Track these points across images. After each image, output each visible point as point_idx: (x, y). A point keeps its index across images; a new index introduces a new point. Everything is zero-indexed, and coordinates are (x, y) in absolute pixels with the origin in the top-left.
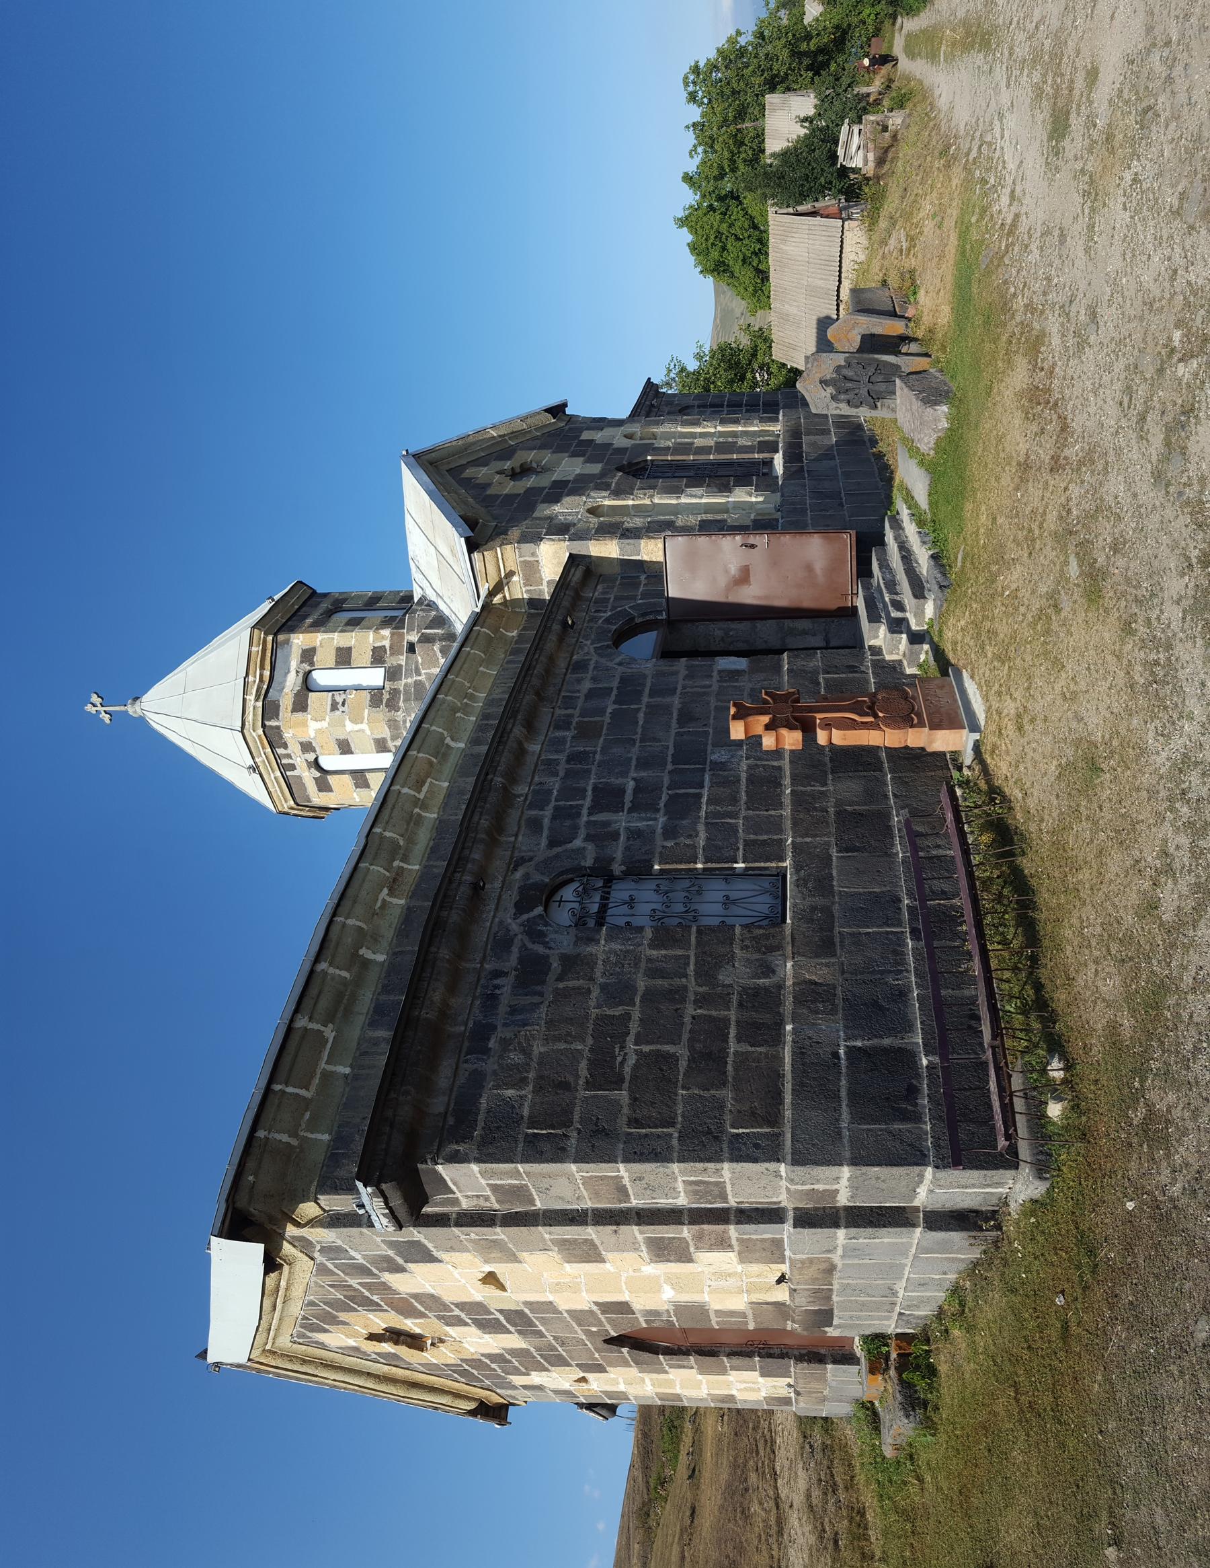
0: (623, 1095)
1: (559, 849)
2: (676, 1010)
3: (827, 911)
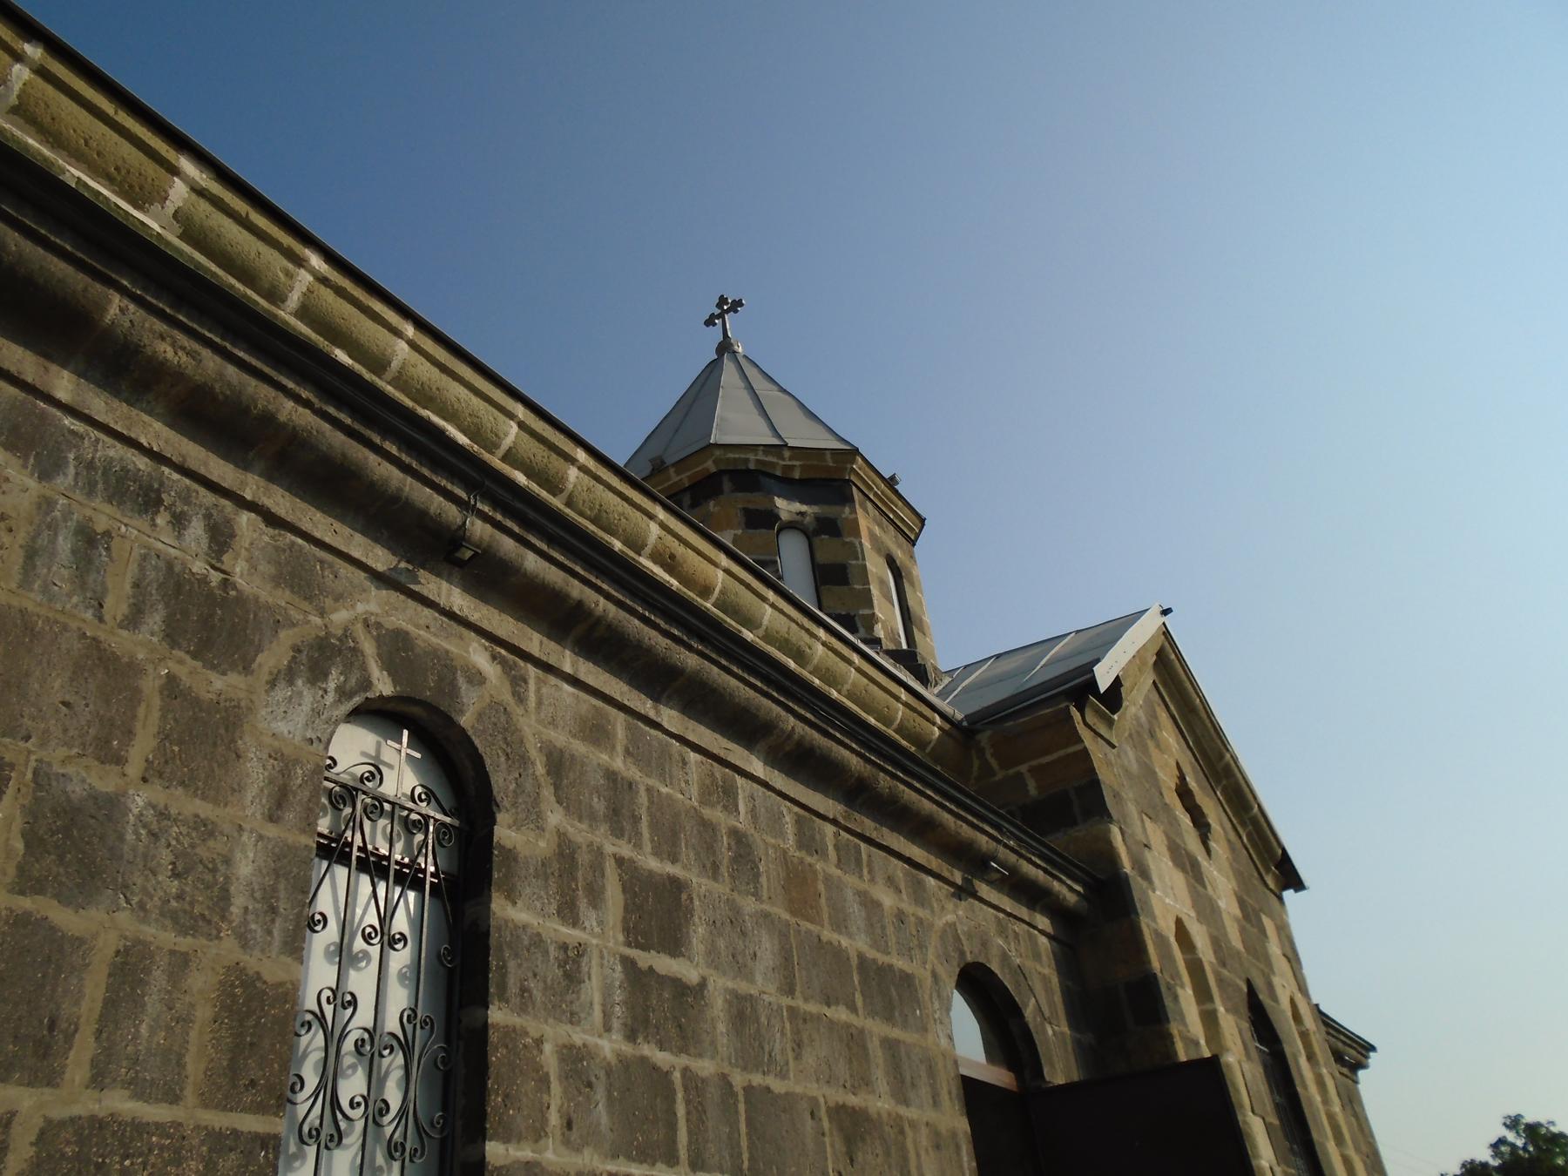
1: (540, 769)
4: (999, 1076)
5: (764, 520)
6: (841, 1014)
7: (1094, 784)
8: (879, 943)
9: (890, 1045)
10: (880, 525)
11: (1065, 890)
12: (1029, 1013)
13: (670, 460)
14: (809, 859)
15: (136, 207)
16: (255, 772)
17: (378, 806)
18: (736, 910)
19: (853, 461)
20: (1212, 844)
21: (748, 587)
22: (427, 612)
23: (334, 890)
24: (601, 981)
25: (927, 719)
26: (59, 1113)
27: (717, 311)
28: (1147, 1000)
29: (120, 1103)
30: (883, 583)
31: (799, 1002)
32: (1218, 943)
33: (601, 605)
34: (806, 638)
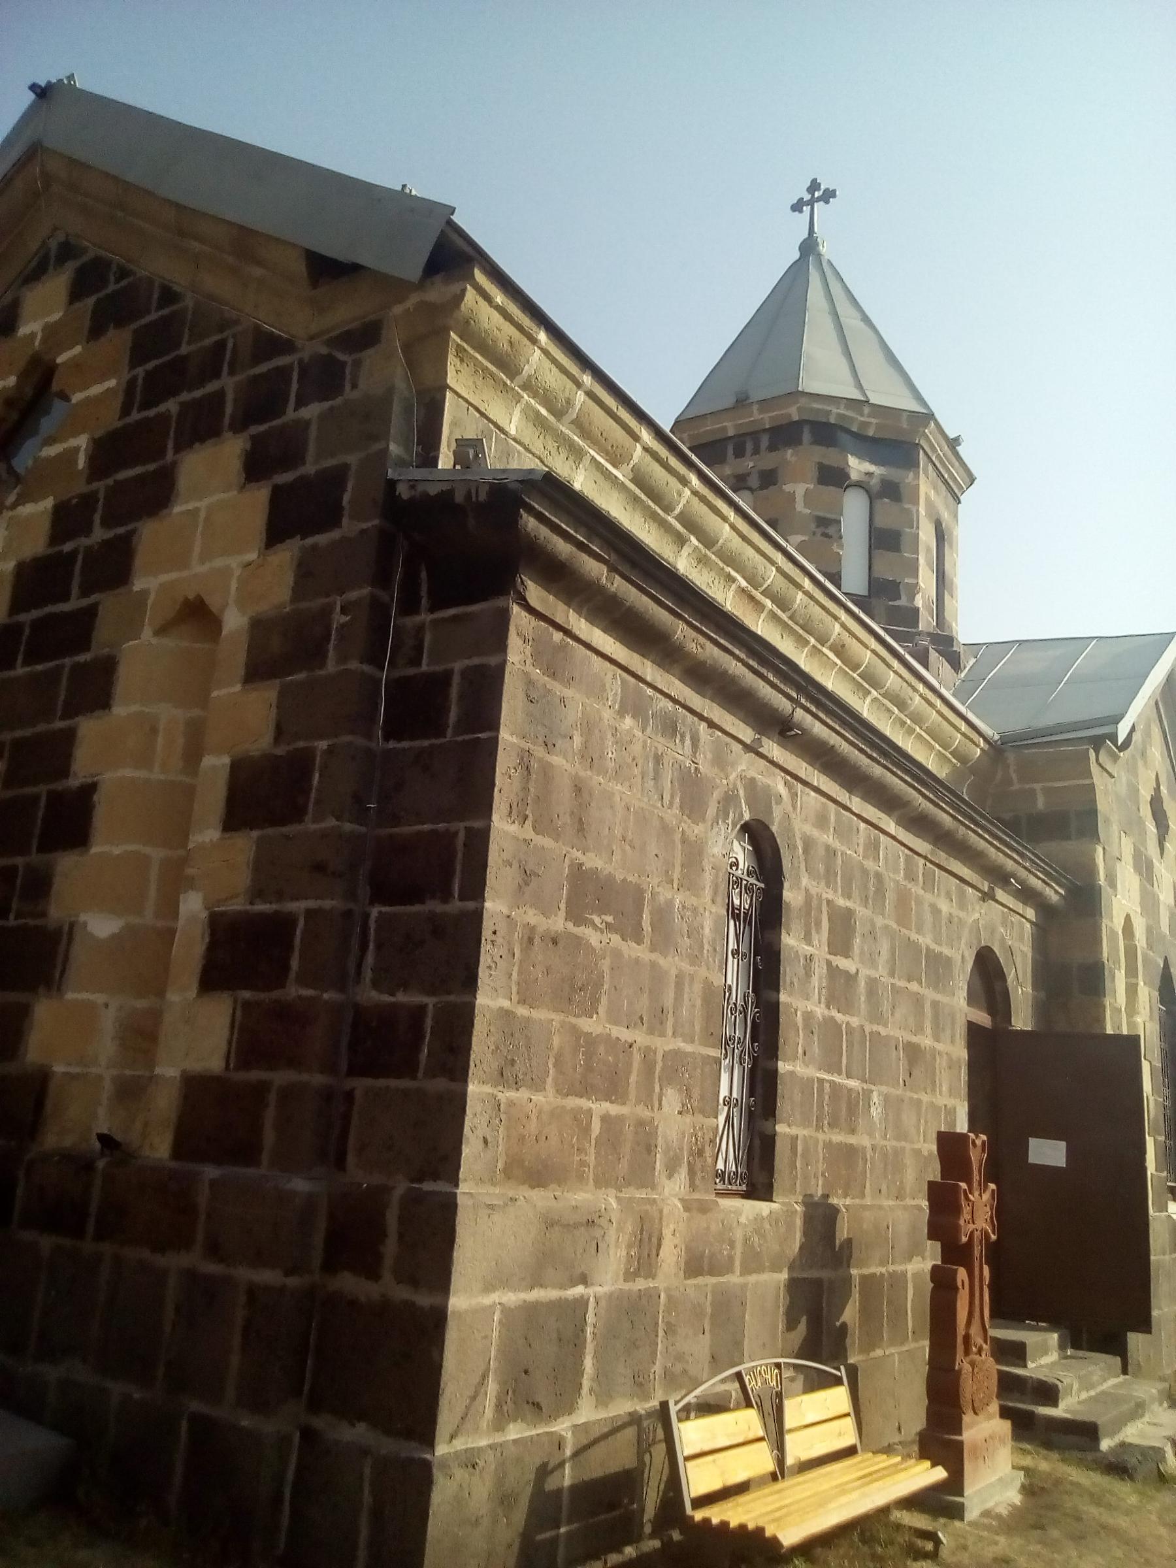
0: (559, 923)
2: (641, 1018)
4: (983, 1019)
6: (914, 987)
7: (1092, 812)
8: (937, 941)
9: (935, 1004)
11: (1052, 893)
12: (1010, 979)
13: (756, 396)
14: (909, 886)
15: (615, 466)
16: (708, 877)
17: (738, 881)
18: (873, 924)
19: (926, 426)
20: (1167, 845)
21: (883, 660)
22: (763, 762)
25: (974, 743)
26: (667, 1048)
27: (807, 197)
28: (1092, 979)
29: (681, 1045)
30: (928, 550)
32: (1149, 930)
33: (844, 747)
34: (910, 690)
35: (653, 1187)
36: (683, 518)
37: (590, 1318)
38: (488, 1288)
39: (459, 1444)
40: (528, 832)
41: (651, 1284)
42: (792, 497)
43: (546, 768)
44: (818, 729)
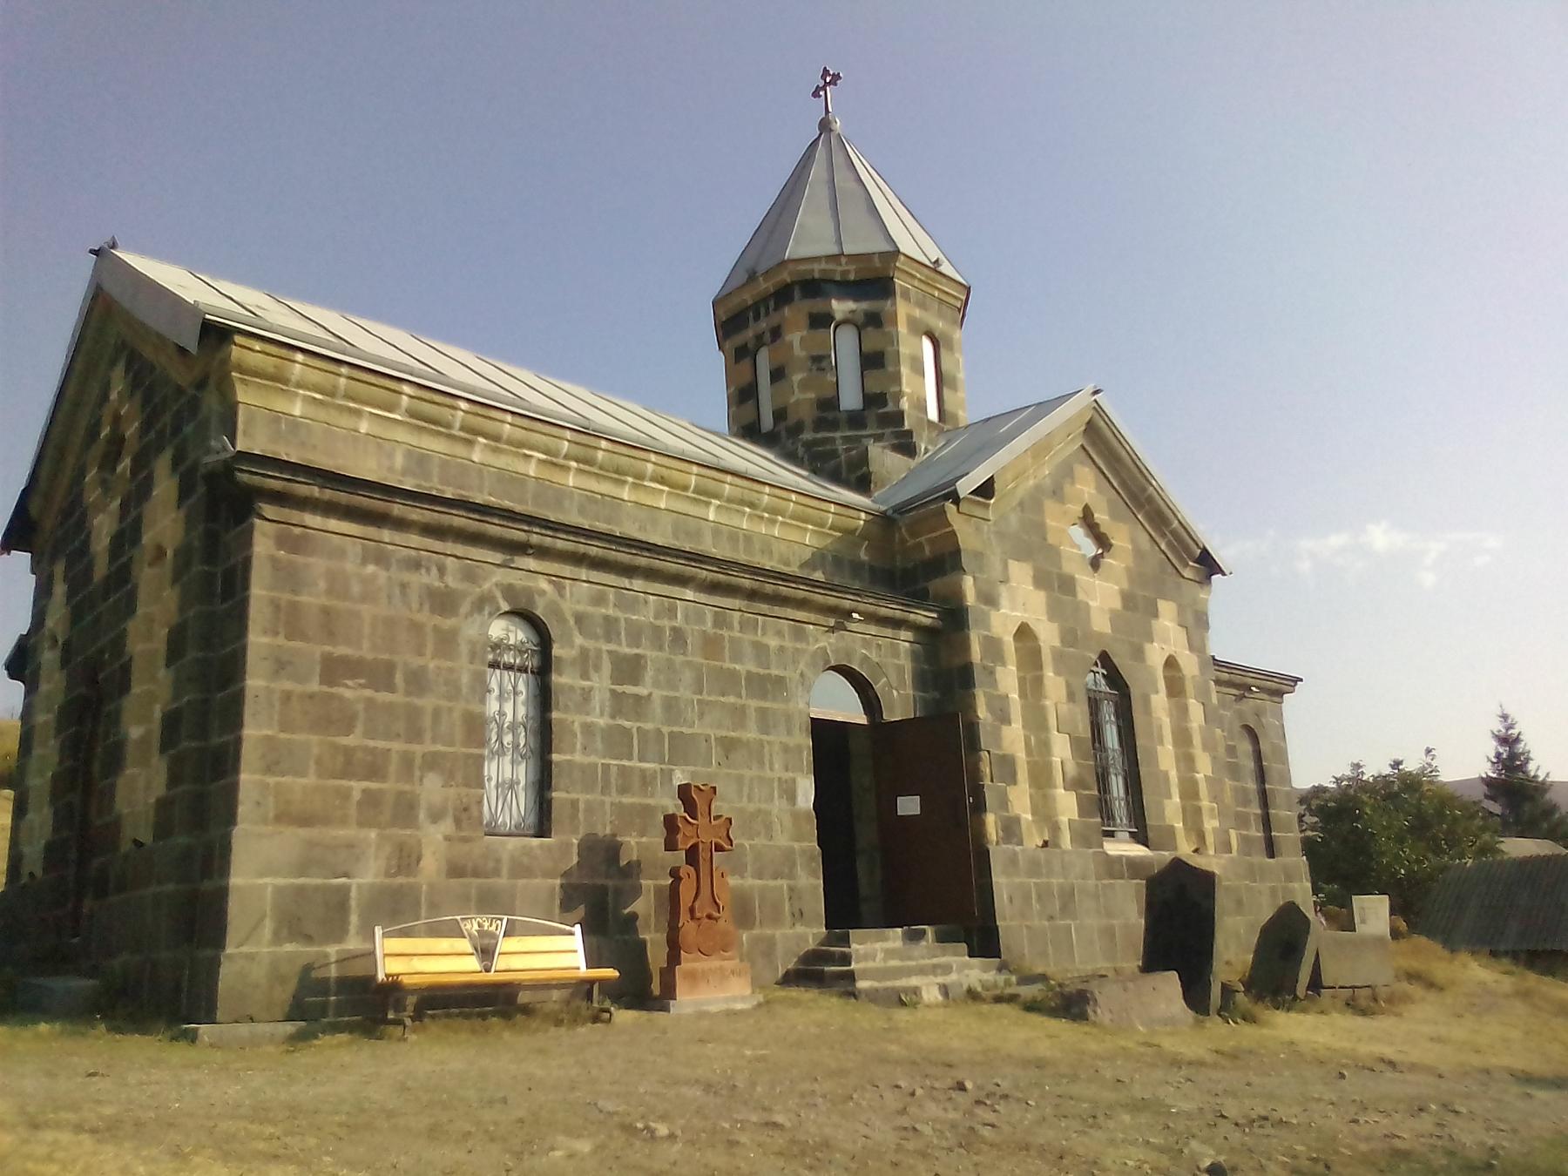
0: (315, 686)
1: (572, 622)
3: (496, 873)
5: (821, 321)
6: (732, 699)
7: (957, 552)
9: (762, 712)
10: (922, 305)
16: (464, 649)
17: (509, 648)
23: (494, 678)
24: (600, 697)
29: (440, 748)
31: (705, 697)
35: (418, 828)
36: (462, 429)
37: (353, 894)
38: (261, 875)
39: (245, 949)
40: (281, 640)
41: (411, 880)
42: (791, 345)
43: (294, 607)
44: (560, 544)
